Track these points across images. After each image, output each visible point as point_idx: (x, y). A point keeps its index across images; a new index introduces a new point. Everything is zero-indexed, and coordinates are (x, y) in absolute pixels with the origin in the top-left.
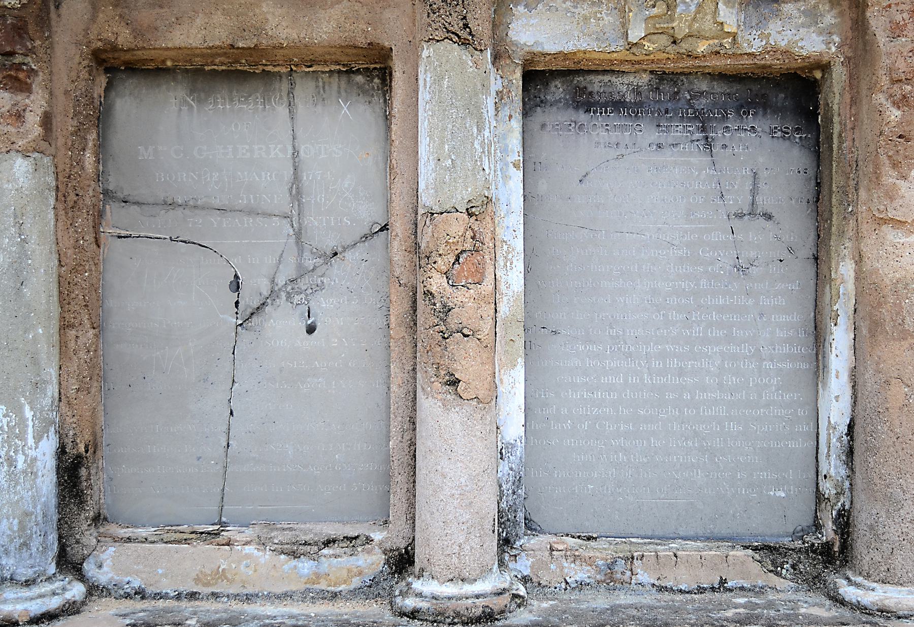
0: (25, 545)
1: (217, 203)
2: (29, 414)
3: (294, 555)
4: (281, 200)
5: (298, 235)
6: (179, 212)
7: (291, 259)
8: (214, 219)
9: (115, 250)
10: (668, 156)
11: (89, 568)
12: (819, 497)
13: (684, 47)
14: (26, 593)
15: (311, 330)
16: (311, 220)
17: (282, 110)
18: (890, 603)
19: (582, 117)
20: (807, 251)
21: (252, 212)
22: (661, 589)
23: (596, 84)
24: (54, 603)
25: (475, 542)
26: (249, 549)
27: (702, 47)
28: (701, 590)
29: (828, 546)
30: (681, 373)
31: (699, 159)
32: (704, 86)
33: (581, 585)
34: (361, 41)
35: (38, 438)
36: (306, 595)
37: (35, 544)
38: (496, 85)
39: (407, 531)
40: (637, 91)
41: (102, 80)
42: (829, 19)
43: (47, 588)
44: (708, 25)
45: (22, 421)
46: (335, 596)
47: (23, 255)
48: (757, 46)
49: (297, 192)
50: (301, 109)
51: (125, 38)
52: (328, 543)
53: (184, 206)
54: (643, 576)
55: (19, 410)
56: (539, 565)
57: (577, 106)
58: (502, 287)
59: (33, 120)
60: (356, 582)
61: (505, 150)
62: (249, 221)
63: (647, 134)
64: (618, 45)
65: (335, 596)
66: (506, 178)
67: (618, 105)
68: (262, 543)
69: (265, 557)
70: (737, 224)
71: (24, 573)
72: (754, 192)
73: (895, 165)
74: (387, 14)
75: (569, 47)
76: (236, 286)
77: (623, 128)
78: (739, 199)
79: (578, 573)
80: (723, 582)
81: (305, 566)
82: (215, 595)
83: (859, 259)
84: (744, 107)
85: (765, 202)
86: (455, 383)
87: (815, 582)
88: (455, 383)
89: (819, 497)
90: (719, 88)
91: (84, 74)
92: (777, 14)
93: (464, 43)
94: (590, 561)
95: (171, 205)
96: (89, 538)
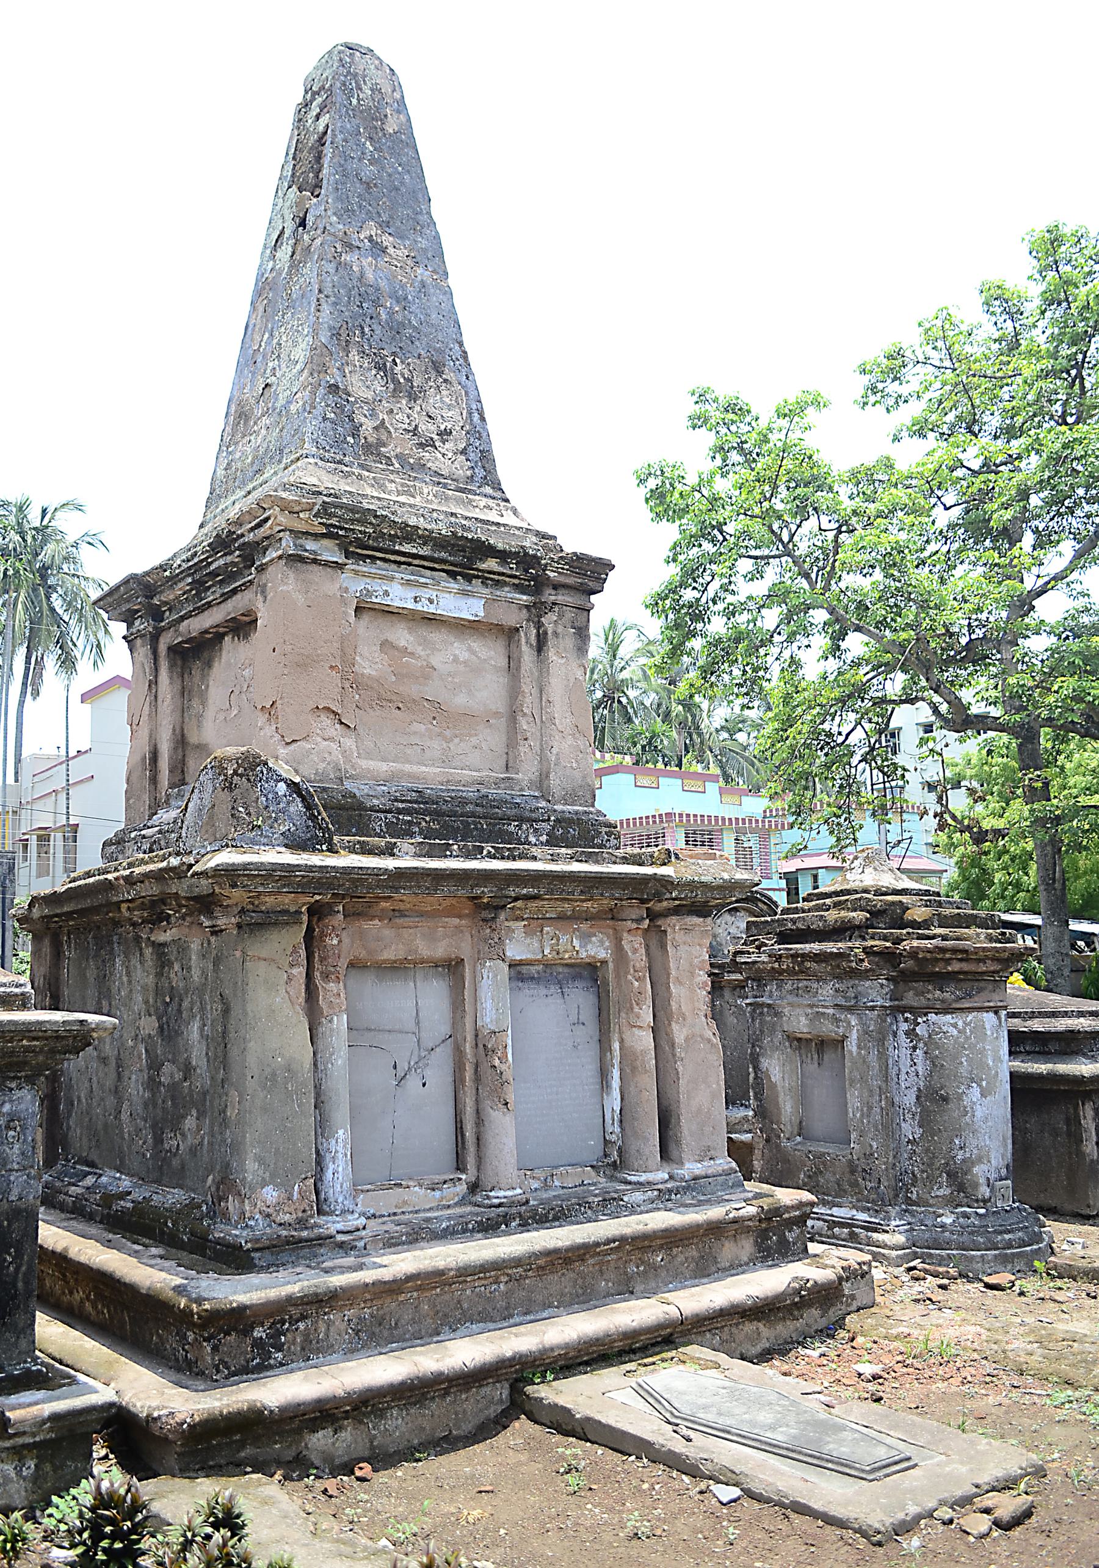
1: (387, 1028)
3: (434, 1190)
4: (411, 1026)
6: (372, 1033)
7: (416, 1053)
8: (386, 1035)
10: (550, 1000)
12: (606, 1142)
13: (561, 956)
15: (424, 1085)
16: (423, 1034)
17: (412, 984)
18: (651, 1179)
20: (597, 1038)
22: (563, 1188)
23: (524, 969)
26: (417, 1189)
29: (615, 1162)
31: (560, 1001)
39: (476, 1173)
40: (538, 972)
42: (607, 944)
46: (449, 1206)
49: (418, 1023)
50: (418, 984)
51: (363, 954)
53: (375, 1030)
54: (557, 1183)
57: (518, 979)
60: (456, 1199)
62: (399, 1035)
65: (449, 1206)
67: (532, 978)
70: (573, 1027)
73: (638, 1004)
74: (463, 945)
76: (395, 1067)
81: (437, 1193)
82: (403, 1213)
83: (622, 1041)
84: (574, 979)
86: (506, 1104)
87: (612, 1178)
89: (606, 1142)
90: (566, 970)
92: (590, 942)
95: (370, 1030)
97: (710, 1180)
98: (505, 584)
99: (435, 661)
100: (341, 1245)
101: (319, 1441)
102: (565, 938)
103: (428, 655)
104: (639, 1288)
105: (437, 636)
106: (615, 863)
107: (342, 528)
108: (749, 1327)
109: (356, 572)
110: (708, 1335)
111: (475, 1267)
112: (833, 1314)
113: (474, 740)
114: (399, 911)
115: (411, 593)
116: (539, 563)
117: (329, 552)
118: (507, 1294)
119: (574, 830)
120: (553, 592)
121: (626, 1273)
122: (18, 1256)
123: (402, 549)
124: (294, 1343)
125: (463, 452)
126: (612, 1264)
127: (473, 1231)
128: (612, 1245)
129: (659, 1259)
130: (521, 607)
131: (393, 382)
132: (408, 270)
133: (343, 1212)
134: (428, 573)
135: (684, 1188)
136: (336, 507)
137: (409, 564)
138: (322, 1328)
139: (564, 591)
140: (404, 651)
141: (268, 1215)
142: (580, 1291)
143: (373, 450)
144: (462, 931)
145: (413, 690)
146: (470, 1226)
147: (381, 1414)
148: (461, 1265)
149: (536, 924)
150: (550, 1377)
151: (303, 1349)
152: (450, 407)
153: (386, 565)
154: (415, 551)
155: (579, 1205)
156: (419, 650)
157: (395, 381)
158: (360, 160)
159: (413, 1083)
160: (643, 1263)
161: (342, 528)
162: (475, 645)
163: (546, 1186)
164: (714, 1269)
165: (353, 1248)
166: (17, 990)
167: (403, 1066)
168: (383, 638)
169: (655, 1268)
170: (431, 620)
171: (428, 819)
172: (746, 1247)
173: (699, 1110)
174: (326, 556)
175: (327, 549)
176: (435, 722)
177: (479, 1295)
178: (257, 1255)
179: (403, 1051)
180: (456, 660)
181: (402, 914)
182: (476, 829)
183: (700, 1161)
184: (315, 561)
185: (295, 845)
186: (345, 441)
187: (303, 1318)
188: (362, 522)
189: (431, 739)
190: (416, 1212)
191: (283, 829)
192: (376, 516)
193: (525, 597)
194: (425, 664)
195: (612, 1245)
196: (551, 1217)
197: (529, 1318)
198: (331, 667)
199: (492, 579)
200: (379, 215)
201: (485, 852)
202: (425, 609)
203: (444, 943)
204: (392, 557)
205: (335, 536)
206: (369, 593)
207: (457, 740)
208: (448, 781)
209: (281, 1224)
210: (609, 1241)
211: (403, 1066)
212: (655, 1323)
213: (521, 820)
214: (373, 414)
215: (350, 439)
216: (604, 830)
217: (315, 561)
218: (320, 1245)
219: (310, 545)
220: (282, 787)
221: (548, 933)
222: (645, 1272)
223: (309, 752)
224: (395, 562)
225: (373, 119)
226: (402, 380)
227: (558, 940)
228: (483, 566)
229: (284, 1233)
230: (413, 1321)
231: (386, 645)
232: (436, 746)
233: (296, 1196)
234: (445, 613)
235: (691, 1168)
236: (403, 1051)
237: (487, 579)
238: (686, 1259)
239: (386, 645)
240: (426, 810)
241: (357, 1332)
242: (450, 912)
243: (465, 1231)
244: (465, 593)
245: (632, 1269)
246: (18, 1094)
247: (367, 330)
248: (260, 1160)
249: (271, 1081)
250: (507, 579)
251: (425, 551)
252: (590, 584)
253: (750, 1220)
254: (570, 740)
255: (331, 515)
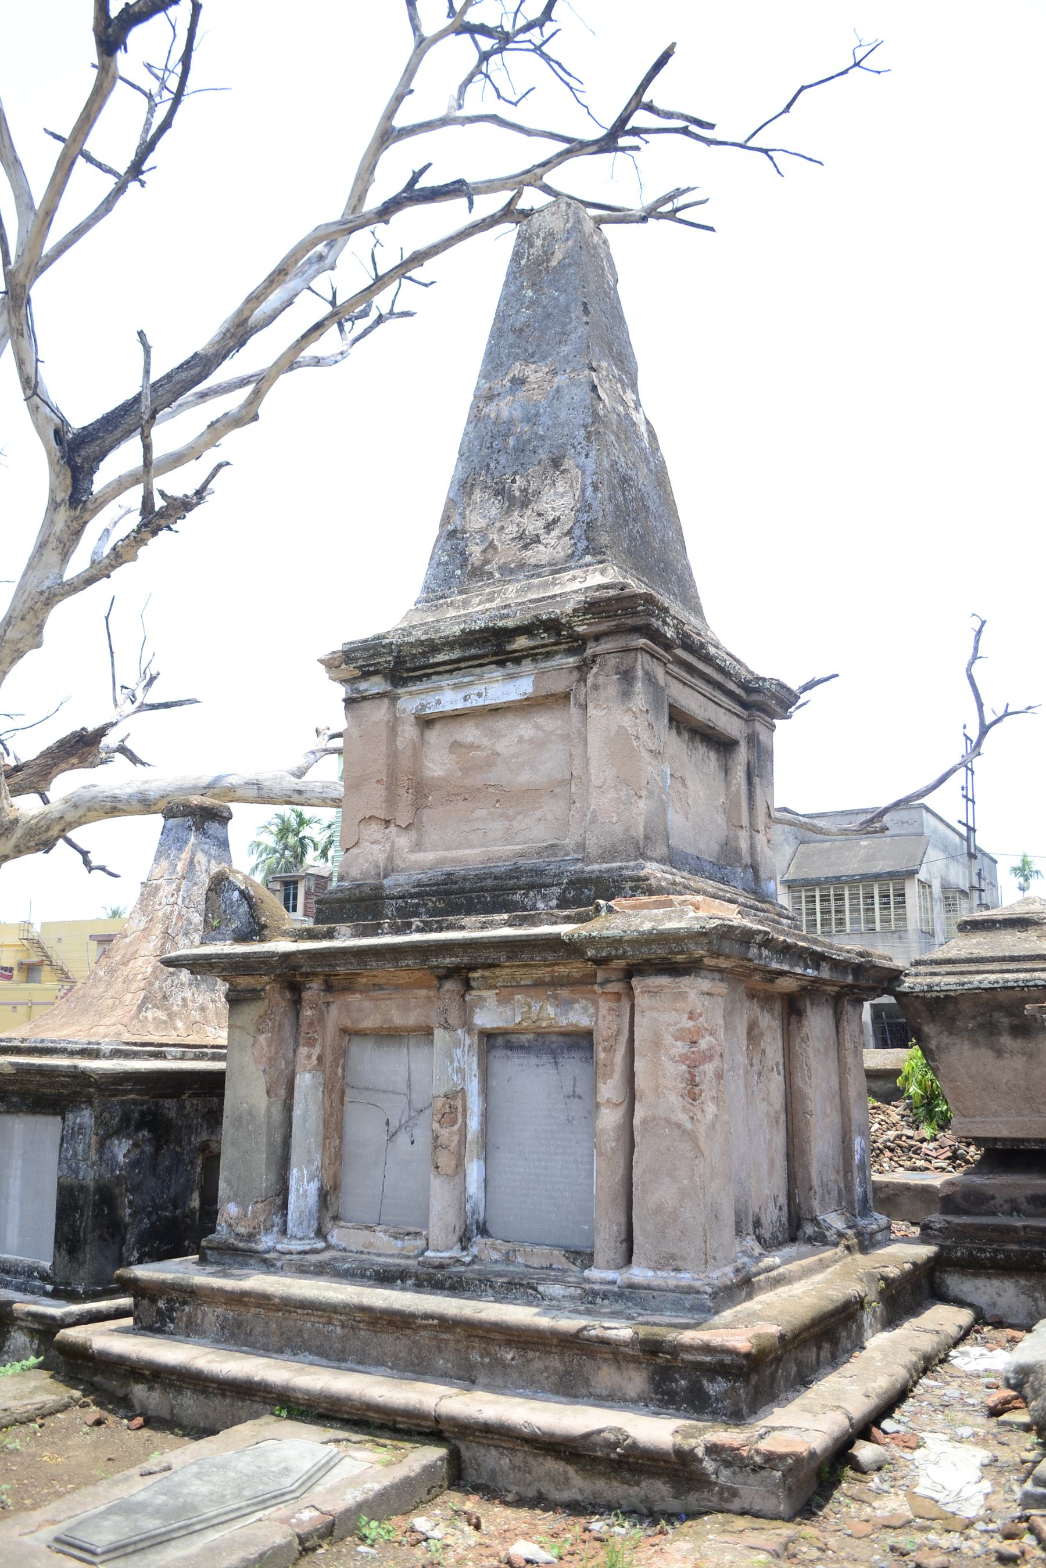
0: (301, 1224)
2: (305, 1172)
3: (396, 1238)
4: (403, 1088)
5: (409, 1102)
7: (406, 1112)
9: (349, 1108)
11: (329, 1237)
13: (538, 1024)
14: (299, 1242)
15: (412, 1143)
16: (414, 1096)
17: (405, 1050)
19: (509, 1053)
21: (394, 1093)
22: (527, 1266)
24: (307, 1248)
25: (443, 1235)
26: (381, 1234)
27: (544, 1024)
28: (542, 1268)
30: (546, 1168)
31: (553, 1071)
32: (554, 1038)
33: (496, 1261)
34: (424, 1025)
35: (309, 1182)
36: (399, 1256)
37: (305, 1223)
38: (468, 1042)
40: (529, 1041)
41: (347, 1038)
43: (308, 1241)
44: (543, 1015)
45: (303, 1175)
46: (408, 1257)
47: (307, 1110)
48: (564, 1023)
49: (409, 1086)
50: (411, 1050)
51: (349, 1025)
52: (408, 1234)
54: (520, 1260)
55: (302, 1171)
56: (481, 1251)
58: (468, 1127)
59: (314, 1057)
61: (471, 1069)
63: (533, 1061)
64: (511, 1025)
65: (408, 1257)
66: (471, 1081)
68: (385, 1232)
69: (386, 1238)
70: (567, 1100)
71: (300, 1235)
72: (574, 1086)
75: (495, 1025)
76: (387, 1123)
77: (524, 1058)
78: (568, 1089)
79: (496, 1256)
80: (551, 1265)
81: (399, 1243)
82: (369, 1253)
84: (571, 1047)
85: (578, 1091)
86: (437, 1167)
88: (437, 1167)
90: (561, 1039)
91: (337, 1038)
92: (572, 1009)
93: (445, 1028)
94: (500, 1251)
95: (367, 1089)
96: (329, 1224)
97: (655, 1293)
98: (556, 653)
99: (501, 747)
100: (265, 1261)
101: (139, 1391)
102: (538, 1006)
103: (493, 744)
104: (482, 1380)
105: (501, 724)
106: (555, 923)
107: (371, 665)
108: (552, 1465)
109: (410, 693)
110: (493, 1452)
111: (295, 1301)
112: (693, 1500)
113: (538, 813)
114: (379, 985)
115: (460, 695)
116: (562, 624)
117: (376, 685)
118: (343, 1339)
119: (590, 890)
120: (594, 644)
121: (467, 1359)
122: (81, 1216)
123: (436, 660)
124: (181, 1320)
125: (569, 532)
126: (452, 1344)
127: (370, 1278)
128: (431, 1321)
129: (509, 1356)
130: (571, 670)
131: (509, 500)
132: (546, 385)
133: (294, 1237)
134: (478, 670)
135: (614, 1294)
136: (354, 652)
137: (460, 669)
138: (200, 1316)
139: (606, 639)
140: (472, 746)
141: (230, 1225)
142: (416, 1361)
143: (478, 573)
144: (432, 1001)
145: (477, 779)
146: (368, 1273)
147: (179, 1390)
148: (284, 1295)
149: (507, 992)
150: (284, 1414)
151: (187, 1327)
152: (562, 495)
153: (440, 677)
154: (447, 658)
155: (480, 1281)
156: (485, 742)
157: (512, 499)
158: (518, 312)
159: (403, 1139)
160: (488, 1354)
161: (371, 665)
162: (542, 720)
163: (507, 1259)
164: (584, 1391)
165: (273, 1265)
166: (96, 1047)
167: (394, 1123)
168: (452, 740)
169: (505, 1366)
170: (496, 710)
171: (434, 899)
172: (636, 1381)
173: (659, 1209)
174: (375, 690)
175: (376, 684)
176: (498, 805)
177: (318, 1331)
178: (209, 1252)
179: (397, 1112)
180: (521, 740)
181: (379, 987)
182: (480, 902)
183: (655, 1269)
184: (364, 698)
185: (241, 937)
186: (453, 576)
187: (185, 1303)
188: (380, 655)
189: (494, 821)
190: (380, 1255)
191: (234, 926)
192: (383, 646)
193: (571, 660)
194: (490, 752)
195: (431, 1321)
196: (447, 1284)
197: (360, 1368)
198: (378, 781)
199: (541, 654)
200: (526, 351)
201: (414, 927)
202: (474, 704)
203: (415, 1013)
204: (441, 669)
205: (376, 673)
206: (423, 707)
207: (520, 817)
208: (489, 859)
209: (237, 1234)
210: (427, 1316)
211: (394, 1123)
212: (402, 1407)
213: (531, 887)
214: (484, 537)
215: (458, 572)
216: (630, 884)
217: (364, 698)
218: (251, 1256)
219: (363, 686)
220: (236, 894)
221: (519, 1001)
222: (490, 1366)
223: (357, 856)
224: (446, 672)
225: (540, 265)
226: (517, 494)
227: (530, 1008)
228: (515, 646)
229: (232, 1241)
230: (264, 1334)
231: (455, 746)
232: (497, 827)
233: (249, 1214)
234: (493, 702)
235: (639, 1273)
236: (397, 1112)
237: (536, 654)
238: (546, 1368)
239: (455, 746)
240: (436, 891)
241: (223, 1328)
242: (418, 985)
243: (363, 1276)
244: (511, 677)
245: (475, 1357)
246: (85, 1112)
247: (492, 466)
248: (229, 1182)
249: (238, 1120)
250: (554, 648)
251: (456, 654)
252: (629, 621)
253: (627, 1346)
254: (612, 794)
255: (356, 659)
